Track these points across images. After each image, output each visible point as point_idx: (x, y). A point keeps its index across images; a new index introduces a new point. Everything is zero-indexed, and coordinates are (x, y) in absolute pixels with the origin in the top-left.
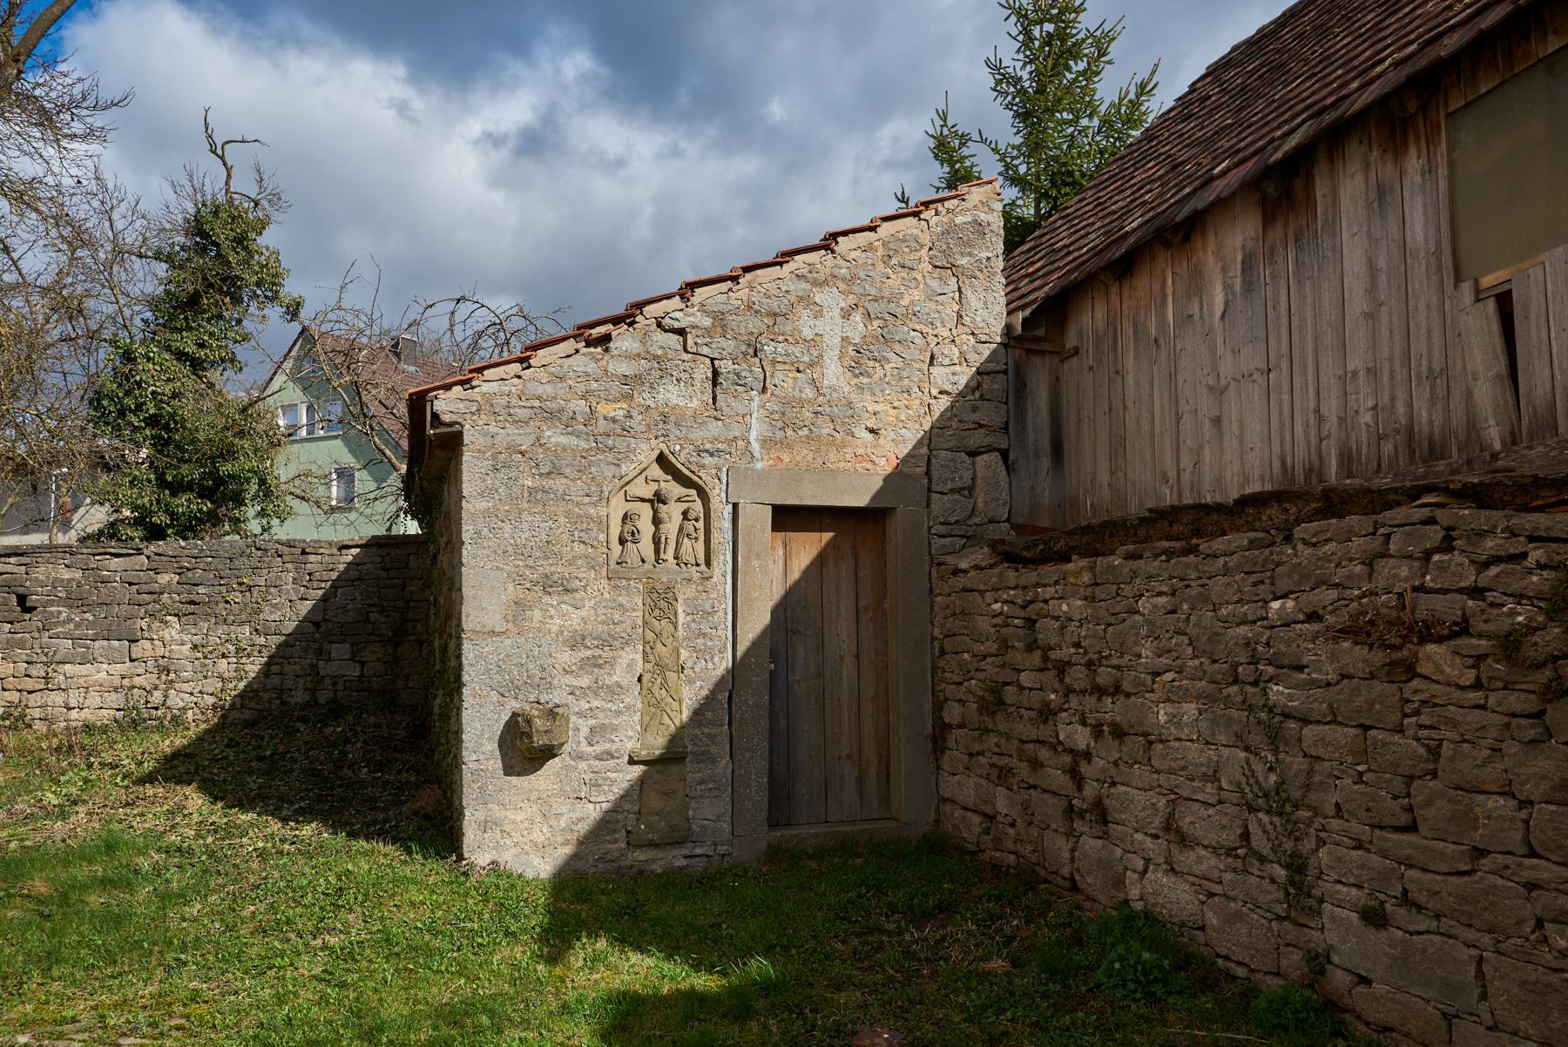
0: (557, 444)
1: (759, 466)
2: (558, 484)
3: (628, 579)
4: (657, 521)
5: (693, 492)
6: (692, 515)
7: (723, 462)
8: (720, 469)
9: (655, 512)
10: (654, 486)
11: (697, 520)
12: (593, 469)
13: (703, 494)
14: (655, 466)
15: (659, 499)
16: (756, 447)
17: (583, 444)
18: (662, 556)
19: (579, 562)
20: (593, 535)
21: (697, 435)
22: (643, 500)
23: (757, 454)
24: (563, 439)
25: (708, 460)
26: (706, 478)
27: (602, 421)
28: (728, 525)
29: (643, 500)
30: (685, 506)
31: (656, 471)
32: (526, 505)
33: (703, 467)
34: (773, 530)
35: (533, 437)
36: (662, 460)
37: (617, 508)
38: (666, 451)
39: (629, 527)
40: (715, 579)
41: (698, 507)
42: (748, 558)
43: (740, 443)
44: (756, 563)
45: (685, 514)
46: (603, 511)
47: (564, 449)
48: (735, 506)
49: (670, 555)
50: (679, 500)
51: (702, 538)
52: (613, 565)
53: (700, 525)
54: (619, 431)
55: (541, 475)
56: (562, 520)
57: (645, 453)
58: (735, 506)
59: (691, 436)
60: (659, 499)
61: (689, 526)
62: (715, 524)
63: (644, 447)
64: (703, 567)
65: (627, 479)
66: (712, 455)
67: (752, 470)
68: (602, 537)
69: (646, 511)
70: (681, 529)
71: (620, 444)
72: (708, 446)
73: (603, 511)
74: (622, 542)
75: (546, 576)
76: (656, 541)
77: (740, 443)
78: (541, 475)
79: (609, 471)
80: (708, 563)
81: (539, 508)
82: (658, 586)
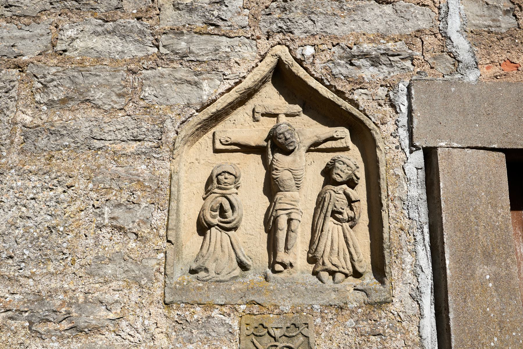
0: (88, 50)
1: (472, 76)
2: (82, 120)
3: (208, 306)
4: (272, 187)
5: (343, 132)
6: (341, 173)
7: (401, 75)
8: (391, 87)
9: (269, 168)
10: (268, 124)
11: (352, 183)
12: (148, 91)
13: (363, 136)
14: (270, 89)
15: (277, 144)
16: (461, 44)
17: (133, 50)
18: (282, 256)
19: (109, 270)
20: (140, 213)
21: (345, 28)
22: (246, 149)
23: (465, 56)
24: (99, 43)
25: (368, 72)
26: (367, 103)
27: (169, 12)
28: (417, 192)
29: (246, 149)
30: (328, 157)
31: (271, 97)
32: (15, 158)
33: (360, 83)
34: (512, 209)
35: (45, 41)
36: (282, 77)
37: (195, 163)
38: (287, 58)
39: (216, 199)
40: (396, 307)
41: (353, 158)
42: (466, 260)
43: (428, 39)
44: (484, 271)
45: (328, 173)
46: (164, 168)
47: (99, 59)
48: (430, 154)
49: (298, 255)
50: (315, 147)
51: (364, 220)
52: (179, 274)
53: (360, 193)
54: (199, 25)
55: (50, 104)
56: (81, 184)
57: (250, 62)
58: (430, 154)
59: (332, 30)
60: (277, 144)
61: (337, 196)
62: (389, 189)
63: (248, 53)
64: (369, 279)
65: (212, 109)
66: (375, 62)
67: (459, 83)
68: (158, 218)
69: (252, 169)
70: (320, 201)
71: (201, 46)
72: (366, 47)
73: (164, 168)
74: (203, 228)
75: (39, 298)
76: (271, 225)
77: (428, 39)
78: (50, 104)
79: (180, 96)
80: (379, 270)
81: (41, 163)
82: (272, 321)
